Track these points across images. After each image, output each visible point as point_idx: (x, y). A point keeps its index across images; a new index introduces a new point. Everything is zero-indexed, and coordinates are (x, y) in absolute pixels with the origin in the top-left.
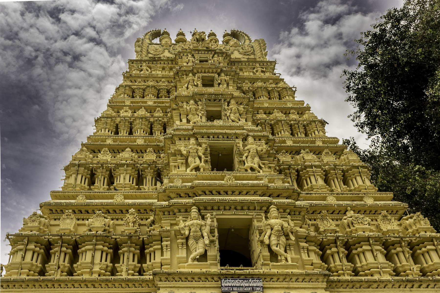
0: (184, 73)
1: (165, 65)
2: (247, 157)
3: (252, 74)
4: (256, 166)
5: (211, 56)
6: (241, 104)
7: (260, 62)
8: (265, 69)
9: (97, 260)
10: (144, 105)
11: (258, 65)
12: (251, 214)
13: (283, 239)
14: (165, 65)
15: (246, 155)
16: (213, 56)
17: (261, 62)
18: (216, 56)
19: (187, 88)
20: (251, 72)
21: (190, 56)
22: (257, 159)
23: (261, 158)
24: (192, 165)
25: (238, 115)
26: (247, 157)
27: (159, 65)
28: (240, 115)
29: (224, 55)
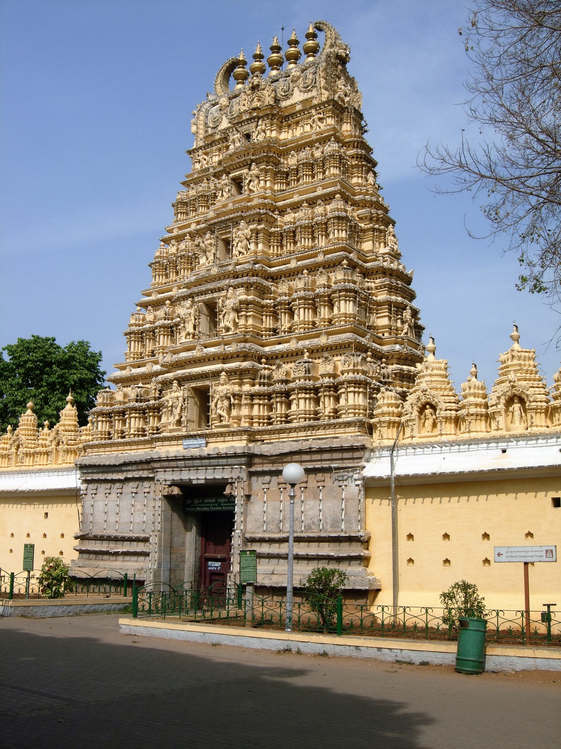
0: (220, 174)
1: (220, 146)
2: (224, 317)
3: (307, 128)
4: (230, 325)
5: (255, 124)
6: (254, 221)
7: (314, 107)
8: (321, 116)
9: (132, 426)
10: (188, 230)
11: (313, 111)
12: (207, 383)
13: (226, 403)
14: (220, 146)
15: (223, 313)
16: (258, 122)
17: (319, 105)
18: (260, 123)
19: (222, 196)
20: (307, 124)
21: (235, 132)
22: (233, 315)
23: (237, 310)
24: (187, 330)
25: (245, 242)
26: (224, 317)
27: (214, 148)
28: (248, 240)
29: (270, 117)
